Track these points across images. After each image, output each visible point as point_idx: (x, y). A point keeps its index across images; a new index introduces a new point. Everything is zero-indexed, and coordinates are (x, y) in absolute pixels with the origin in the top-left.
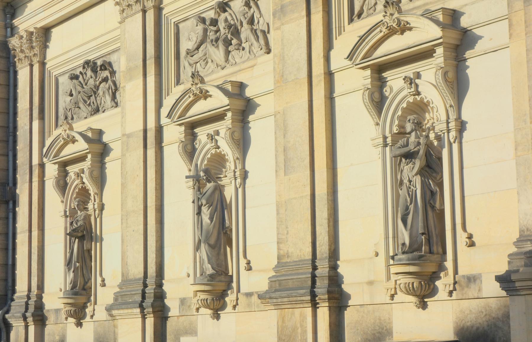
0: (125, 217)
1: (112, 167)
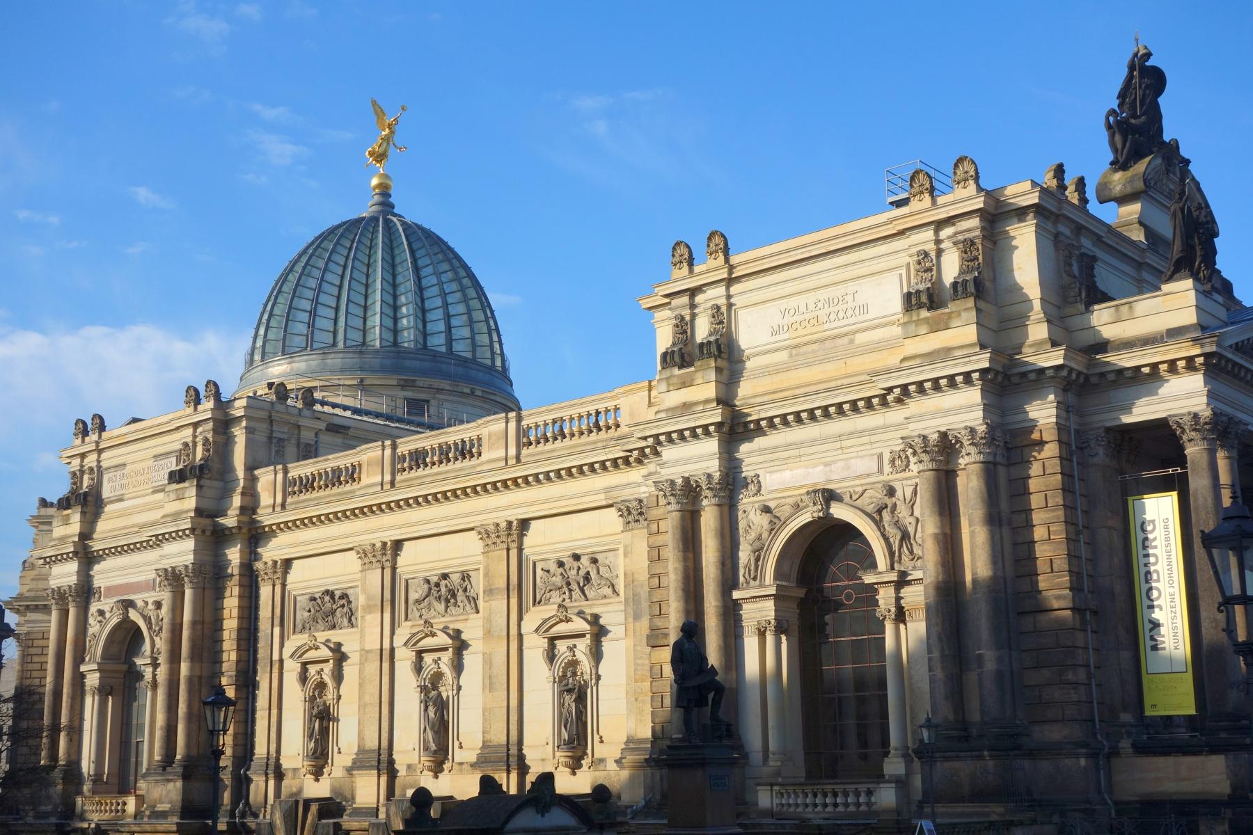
0: (362, 707)
1: (349, 670)
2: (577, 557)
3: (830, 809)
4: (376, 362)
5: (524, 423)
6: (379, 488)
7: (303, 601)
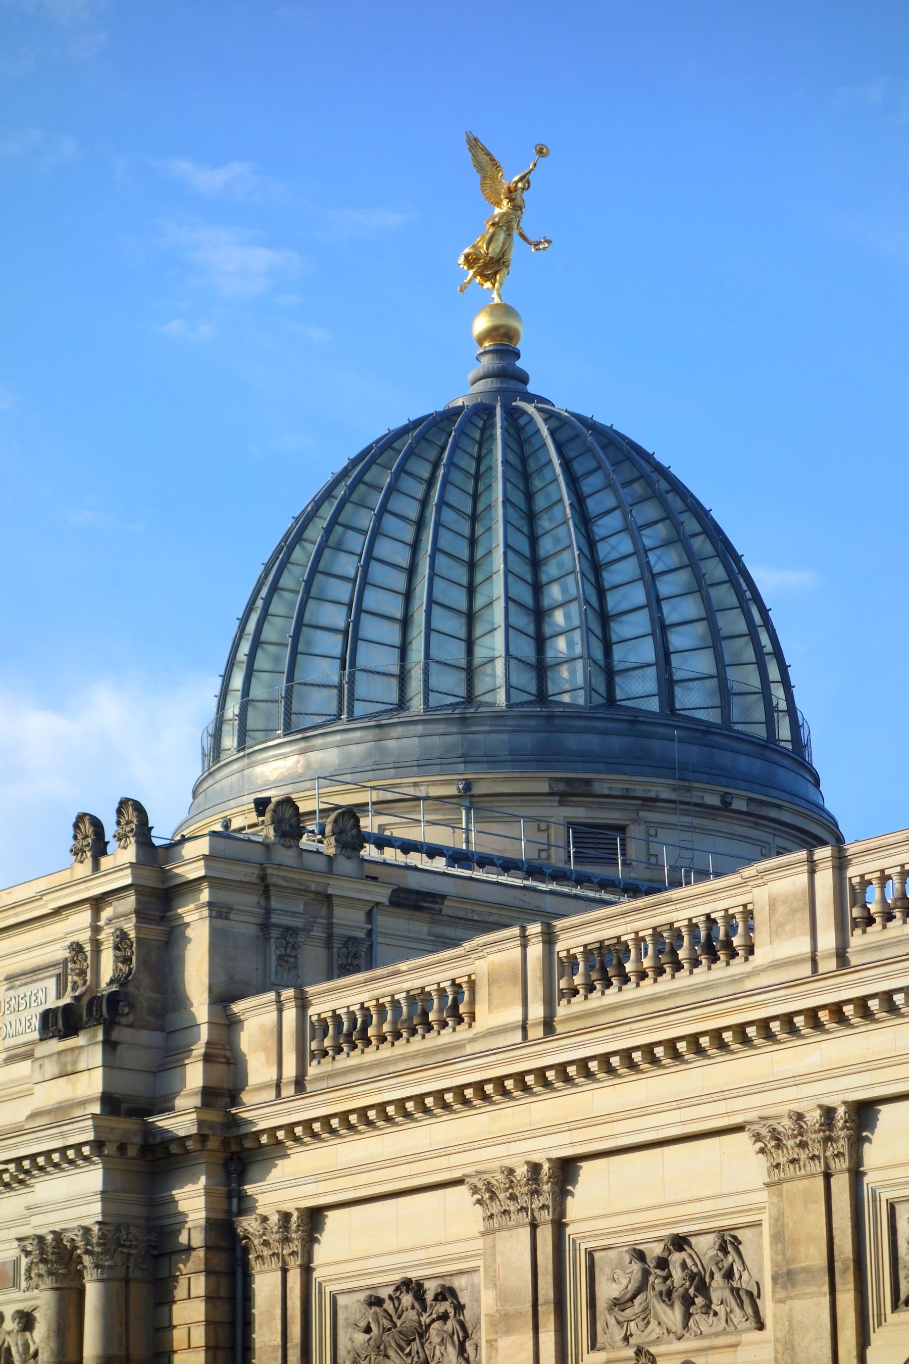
4: (501, 740)
5: (853, 872)
6: (517, 1037)
7: (352, 1307)
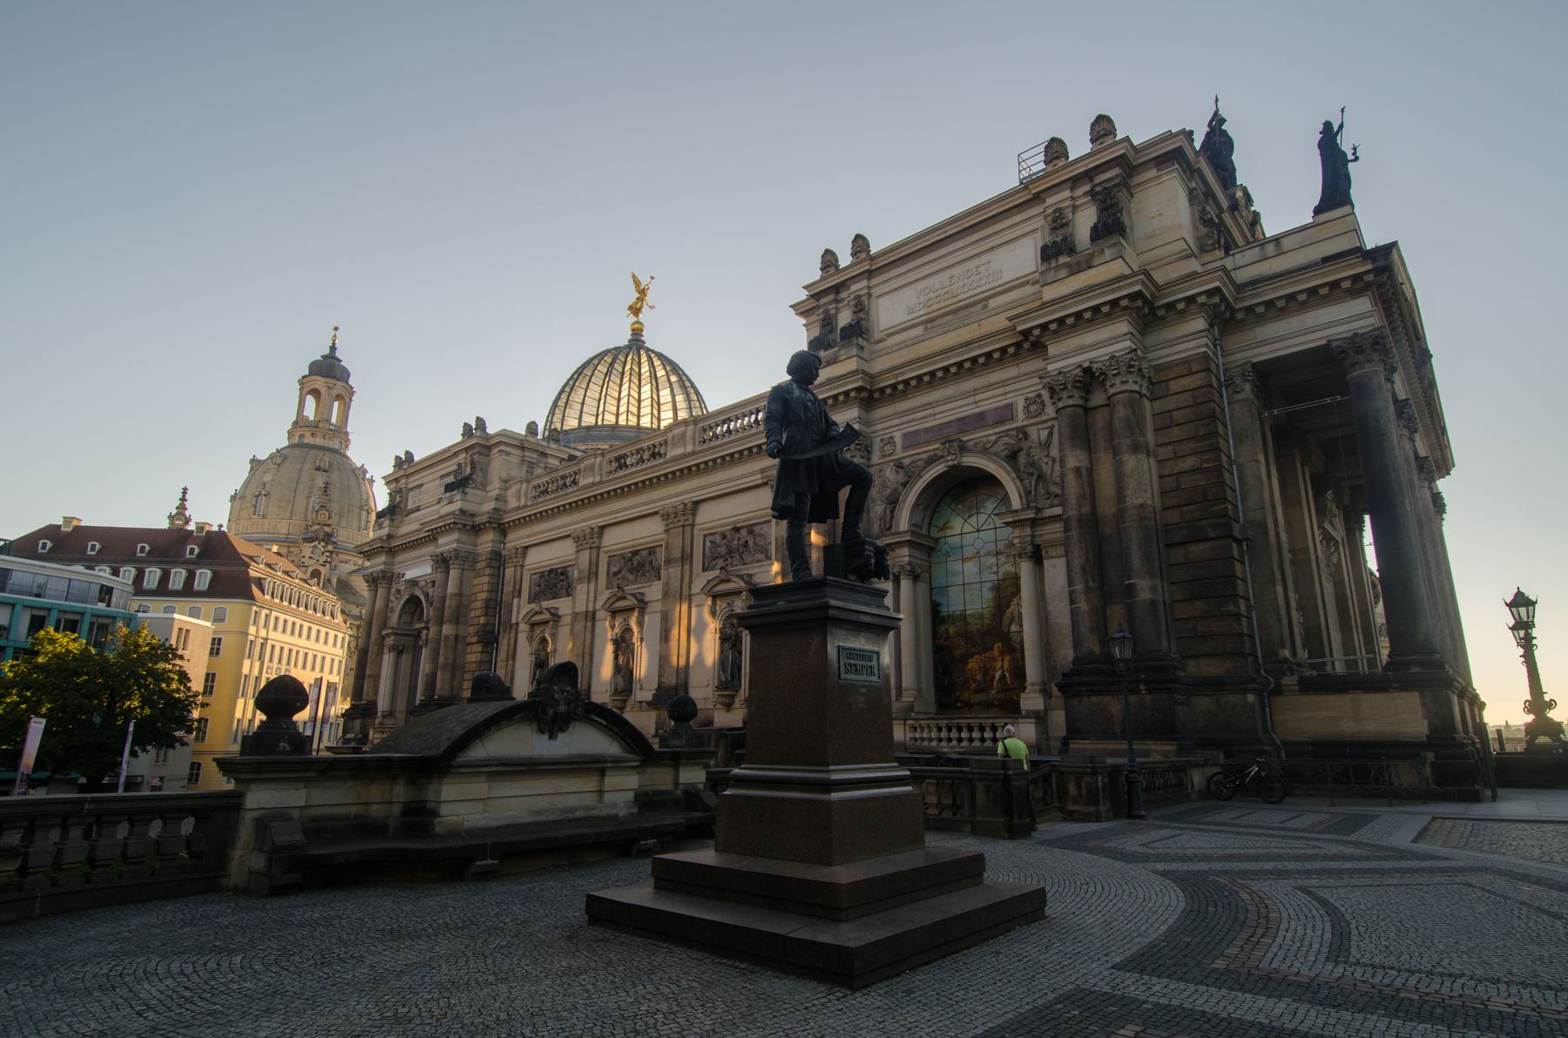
2: (737, 529)
3: (965, 744)
